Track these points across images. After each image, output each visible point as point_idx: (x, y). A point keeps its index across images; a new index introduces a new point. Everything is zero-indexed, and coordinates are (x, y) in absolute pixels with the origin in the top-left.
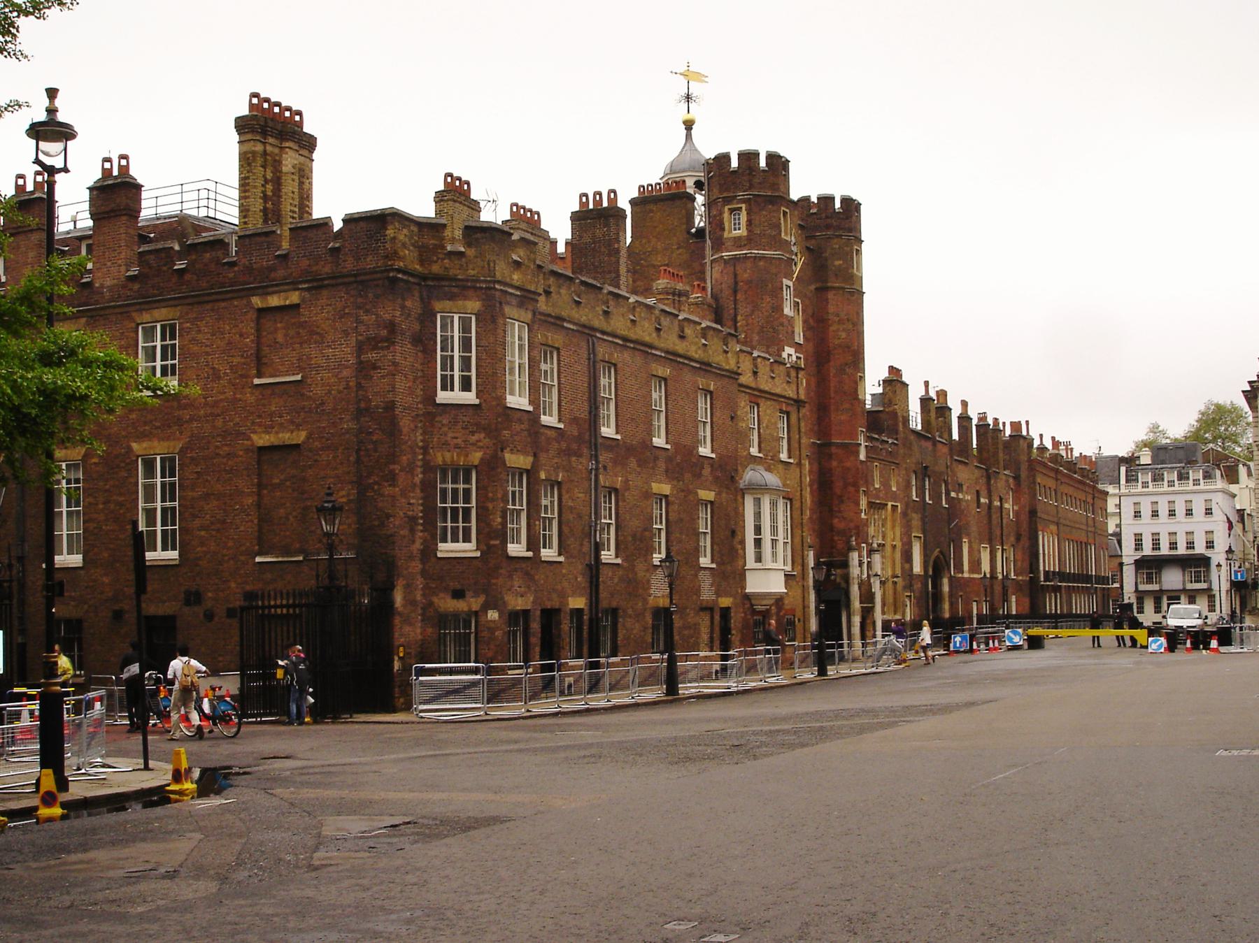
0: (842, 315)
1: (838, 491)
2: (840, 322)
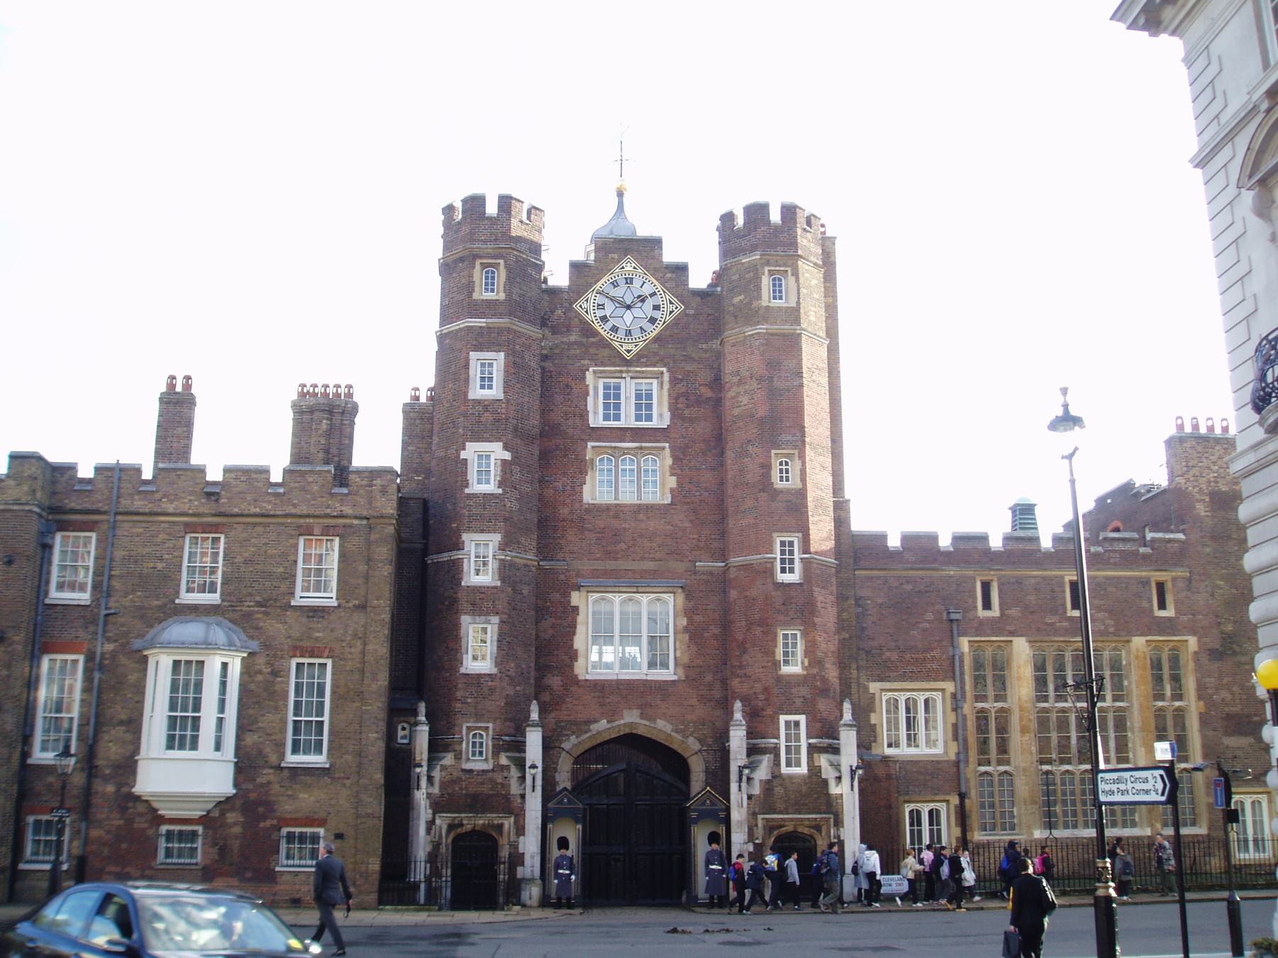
0: (745, 374)
1: (739, 636)
2: (741, 382)
